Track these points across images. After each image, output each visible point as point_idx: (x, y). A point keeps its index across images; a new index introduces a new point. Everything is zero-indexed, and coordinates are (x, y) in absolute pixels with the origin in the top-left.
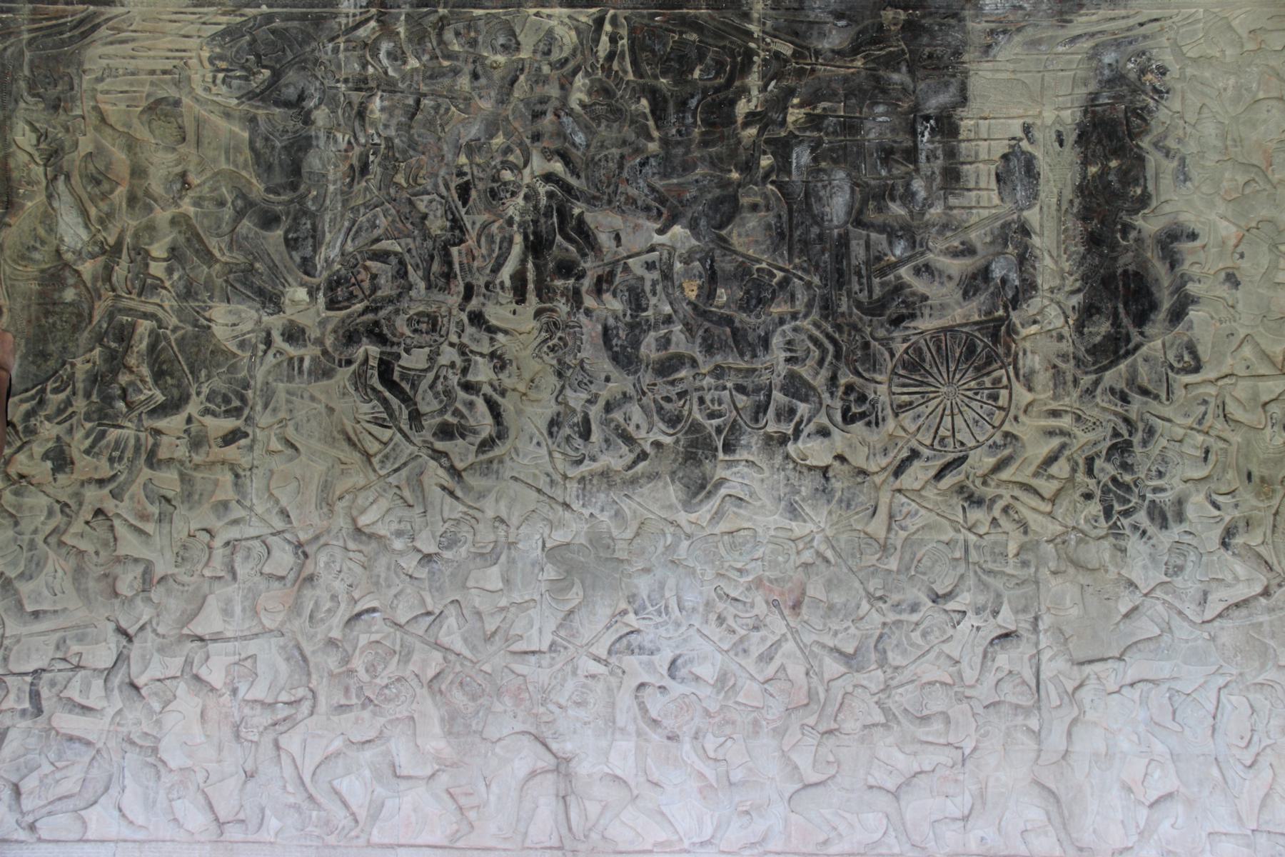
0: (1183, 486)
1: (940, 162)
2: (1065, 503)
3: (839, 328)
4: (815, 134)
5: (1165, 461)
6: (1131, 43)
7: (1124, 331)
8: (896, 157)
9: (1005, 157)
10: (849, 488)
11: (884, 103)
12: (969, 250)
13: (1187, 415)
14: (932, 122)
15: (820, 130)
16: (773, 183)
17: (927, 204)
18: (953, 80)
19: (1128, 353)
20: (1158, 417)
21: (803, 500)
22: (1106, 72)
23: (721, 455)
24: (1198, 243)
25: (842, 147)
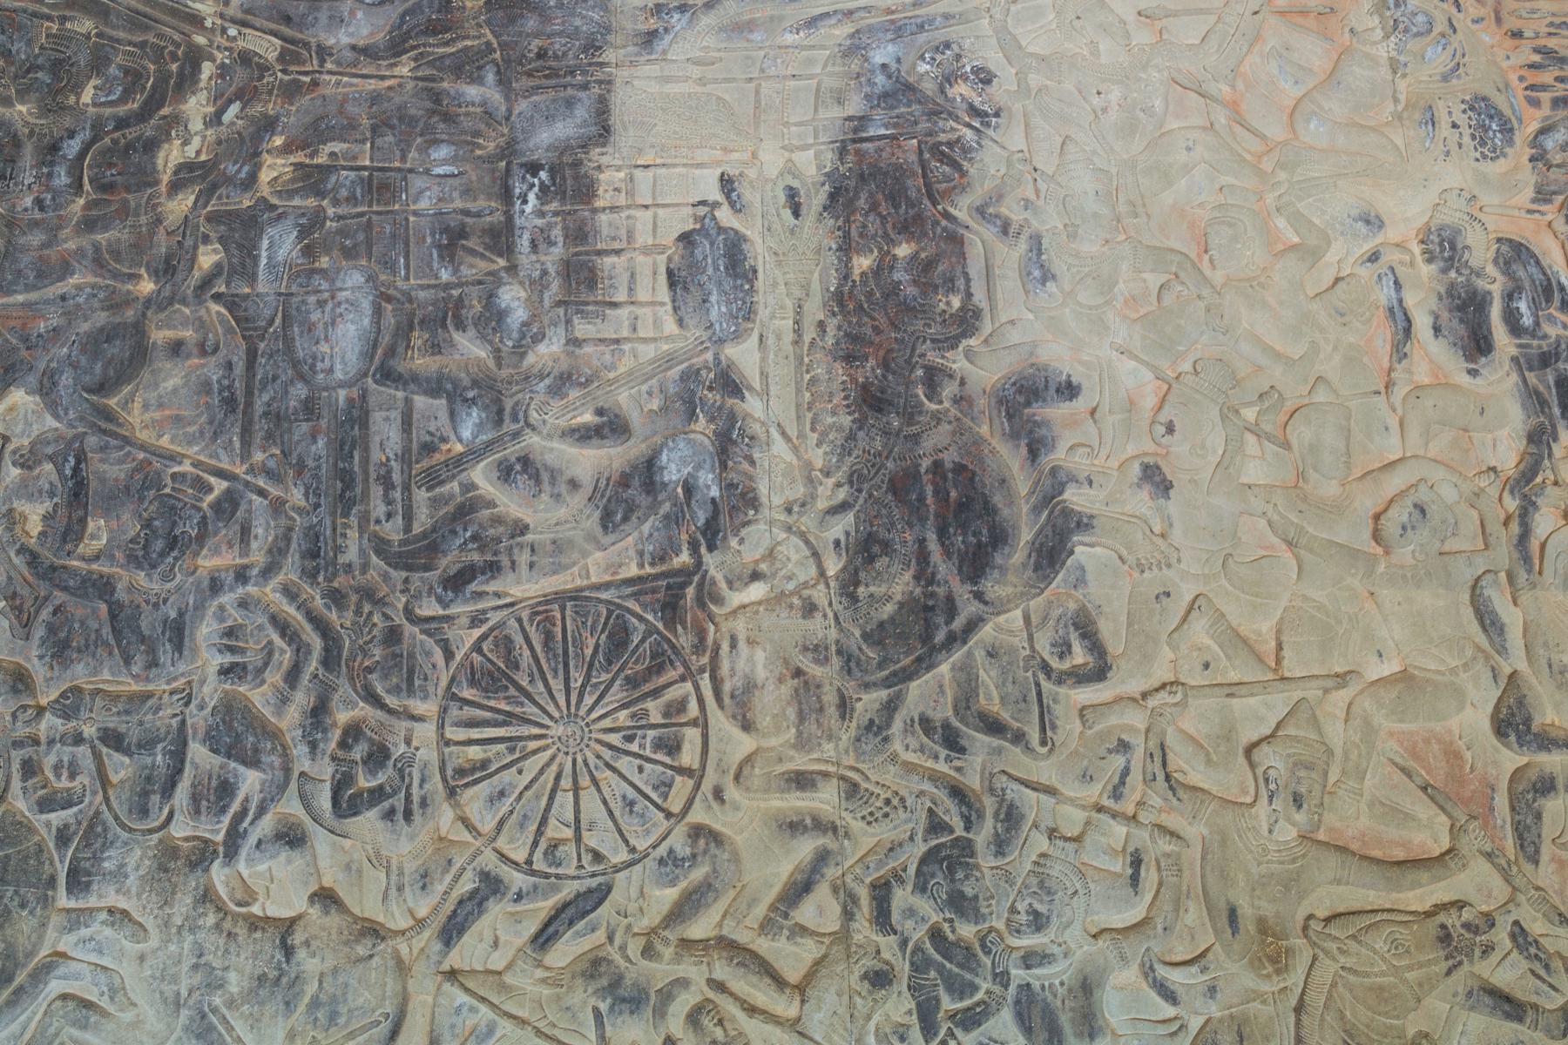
0: (1089, 947)
1: (558, 251)
2: (830, 998)
3: (336, 598)
4: (311, 202)
5: (1045, 888)
6: (921, 27)
7: (941, 591)
8: (470, 244)
9: (686, 238)
10: (335, 971)
11: (449, 142)
12: (611, 427)
13: (1087, 777)
14: (543, 175)
15: (321, 194)
16: (217, 297)
17: (530, 336)
18: (582, 94)
19: (952, 640)
20: (1026, 784)
21: (231, 1004)
22: (880, 79)
23: (63, 900)
24: (1081, 404)
25: (359, 220)
